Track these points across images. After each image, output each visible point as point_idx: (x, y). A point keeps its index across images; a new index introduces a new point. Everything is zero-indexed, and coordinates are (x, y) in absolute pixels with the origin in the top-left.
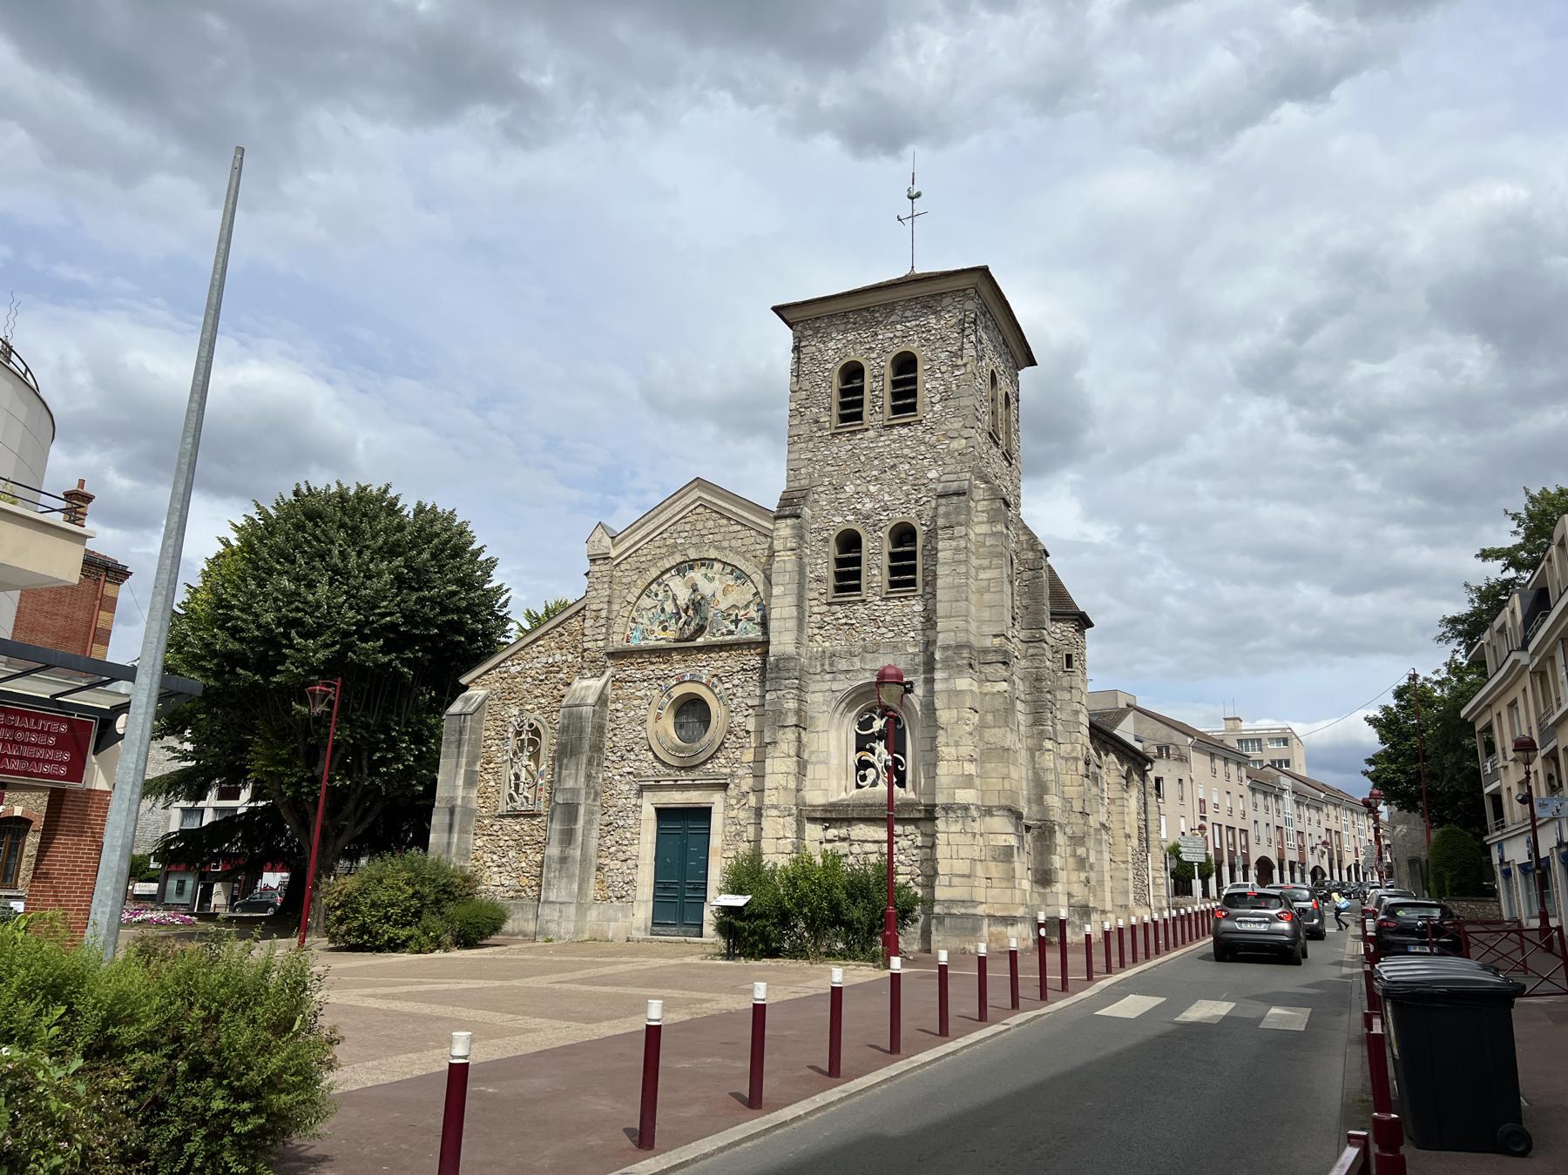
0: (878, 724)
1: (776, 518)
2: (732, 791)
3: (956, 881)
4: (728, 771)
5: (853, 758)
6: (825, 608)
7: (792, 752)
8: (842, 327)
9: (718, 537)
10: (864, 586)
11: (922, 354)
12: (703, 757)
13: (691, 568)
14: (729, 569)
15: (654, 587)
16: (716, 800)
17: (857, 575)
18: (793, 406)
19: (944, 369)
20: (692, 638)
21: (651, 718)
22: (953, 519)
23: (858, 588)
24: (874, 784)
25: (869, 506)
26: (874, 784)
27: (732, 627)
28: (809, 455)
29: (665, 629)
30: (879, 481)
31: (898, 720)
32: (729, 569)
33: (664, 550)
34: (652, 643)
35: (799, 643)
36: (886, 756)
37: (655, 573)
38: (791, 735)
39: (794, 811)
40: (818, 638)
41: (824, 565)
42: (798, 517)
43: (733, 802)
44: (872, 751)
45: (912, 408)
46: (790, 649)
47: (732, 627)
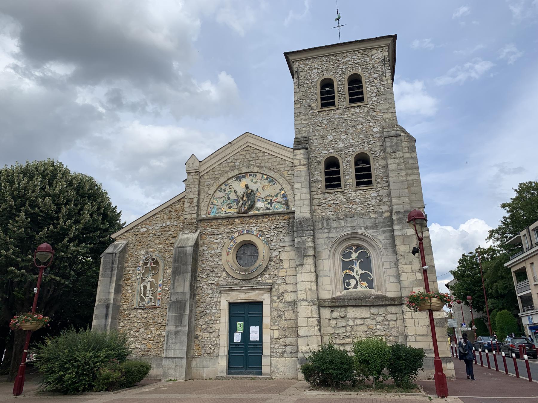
0: (354, 256)
1: (294, 150)
3: (419, 338)
4: (270, 281)
5: (341, 274)
6: (320, 196)
7: (313, 270)
8: (320, 63)
9: (259, 161)
10: (342, 185)
11: (364, 75)
12: (256, 274)
13: (244, 177)
14: (265, 177)
15: (223, 187)
16: (265, 298)
17: (339, 179)
18: (296, 99)
19: (376, 81)
20: (246, 212)
21: (224, 254)
22: (395, 148)
23: (339, 186)
24: (355, 287)
25: (341, 145)
26: (355, 287)
27: (269, 206)
28: (307, 122)
29: (230, 207)
30: (344, 134)
31: (365, 253)
32: (265, 177)
33: (229, 168)
34: (223, 215)
35: (312, 211)
36: (361, 272)
37: (223, 179)
38: (310, 261)
39: (317, 302)
40: (319, 211)
41: (320, 175)
42: (307, 149)
43: (275, 298)
44: (352, 269)
45: (362, 100)
46: (308, 215)
47: (269, 206)
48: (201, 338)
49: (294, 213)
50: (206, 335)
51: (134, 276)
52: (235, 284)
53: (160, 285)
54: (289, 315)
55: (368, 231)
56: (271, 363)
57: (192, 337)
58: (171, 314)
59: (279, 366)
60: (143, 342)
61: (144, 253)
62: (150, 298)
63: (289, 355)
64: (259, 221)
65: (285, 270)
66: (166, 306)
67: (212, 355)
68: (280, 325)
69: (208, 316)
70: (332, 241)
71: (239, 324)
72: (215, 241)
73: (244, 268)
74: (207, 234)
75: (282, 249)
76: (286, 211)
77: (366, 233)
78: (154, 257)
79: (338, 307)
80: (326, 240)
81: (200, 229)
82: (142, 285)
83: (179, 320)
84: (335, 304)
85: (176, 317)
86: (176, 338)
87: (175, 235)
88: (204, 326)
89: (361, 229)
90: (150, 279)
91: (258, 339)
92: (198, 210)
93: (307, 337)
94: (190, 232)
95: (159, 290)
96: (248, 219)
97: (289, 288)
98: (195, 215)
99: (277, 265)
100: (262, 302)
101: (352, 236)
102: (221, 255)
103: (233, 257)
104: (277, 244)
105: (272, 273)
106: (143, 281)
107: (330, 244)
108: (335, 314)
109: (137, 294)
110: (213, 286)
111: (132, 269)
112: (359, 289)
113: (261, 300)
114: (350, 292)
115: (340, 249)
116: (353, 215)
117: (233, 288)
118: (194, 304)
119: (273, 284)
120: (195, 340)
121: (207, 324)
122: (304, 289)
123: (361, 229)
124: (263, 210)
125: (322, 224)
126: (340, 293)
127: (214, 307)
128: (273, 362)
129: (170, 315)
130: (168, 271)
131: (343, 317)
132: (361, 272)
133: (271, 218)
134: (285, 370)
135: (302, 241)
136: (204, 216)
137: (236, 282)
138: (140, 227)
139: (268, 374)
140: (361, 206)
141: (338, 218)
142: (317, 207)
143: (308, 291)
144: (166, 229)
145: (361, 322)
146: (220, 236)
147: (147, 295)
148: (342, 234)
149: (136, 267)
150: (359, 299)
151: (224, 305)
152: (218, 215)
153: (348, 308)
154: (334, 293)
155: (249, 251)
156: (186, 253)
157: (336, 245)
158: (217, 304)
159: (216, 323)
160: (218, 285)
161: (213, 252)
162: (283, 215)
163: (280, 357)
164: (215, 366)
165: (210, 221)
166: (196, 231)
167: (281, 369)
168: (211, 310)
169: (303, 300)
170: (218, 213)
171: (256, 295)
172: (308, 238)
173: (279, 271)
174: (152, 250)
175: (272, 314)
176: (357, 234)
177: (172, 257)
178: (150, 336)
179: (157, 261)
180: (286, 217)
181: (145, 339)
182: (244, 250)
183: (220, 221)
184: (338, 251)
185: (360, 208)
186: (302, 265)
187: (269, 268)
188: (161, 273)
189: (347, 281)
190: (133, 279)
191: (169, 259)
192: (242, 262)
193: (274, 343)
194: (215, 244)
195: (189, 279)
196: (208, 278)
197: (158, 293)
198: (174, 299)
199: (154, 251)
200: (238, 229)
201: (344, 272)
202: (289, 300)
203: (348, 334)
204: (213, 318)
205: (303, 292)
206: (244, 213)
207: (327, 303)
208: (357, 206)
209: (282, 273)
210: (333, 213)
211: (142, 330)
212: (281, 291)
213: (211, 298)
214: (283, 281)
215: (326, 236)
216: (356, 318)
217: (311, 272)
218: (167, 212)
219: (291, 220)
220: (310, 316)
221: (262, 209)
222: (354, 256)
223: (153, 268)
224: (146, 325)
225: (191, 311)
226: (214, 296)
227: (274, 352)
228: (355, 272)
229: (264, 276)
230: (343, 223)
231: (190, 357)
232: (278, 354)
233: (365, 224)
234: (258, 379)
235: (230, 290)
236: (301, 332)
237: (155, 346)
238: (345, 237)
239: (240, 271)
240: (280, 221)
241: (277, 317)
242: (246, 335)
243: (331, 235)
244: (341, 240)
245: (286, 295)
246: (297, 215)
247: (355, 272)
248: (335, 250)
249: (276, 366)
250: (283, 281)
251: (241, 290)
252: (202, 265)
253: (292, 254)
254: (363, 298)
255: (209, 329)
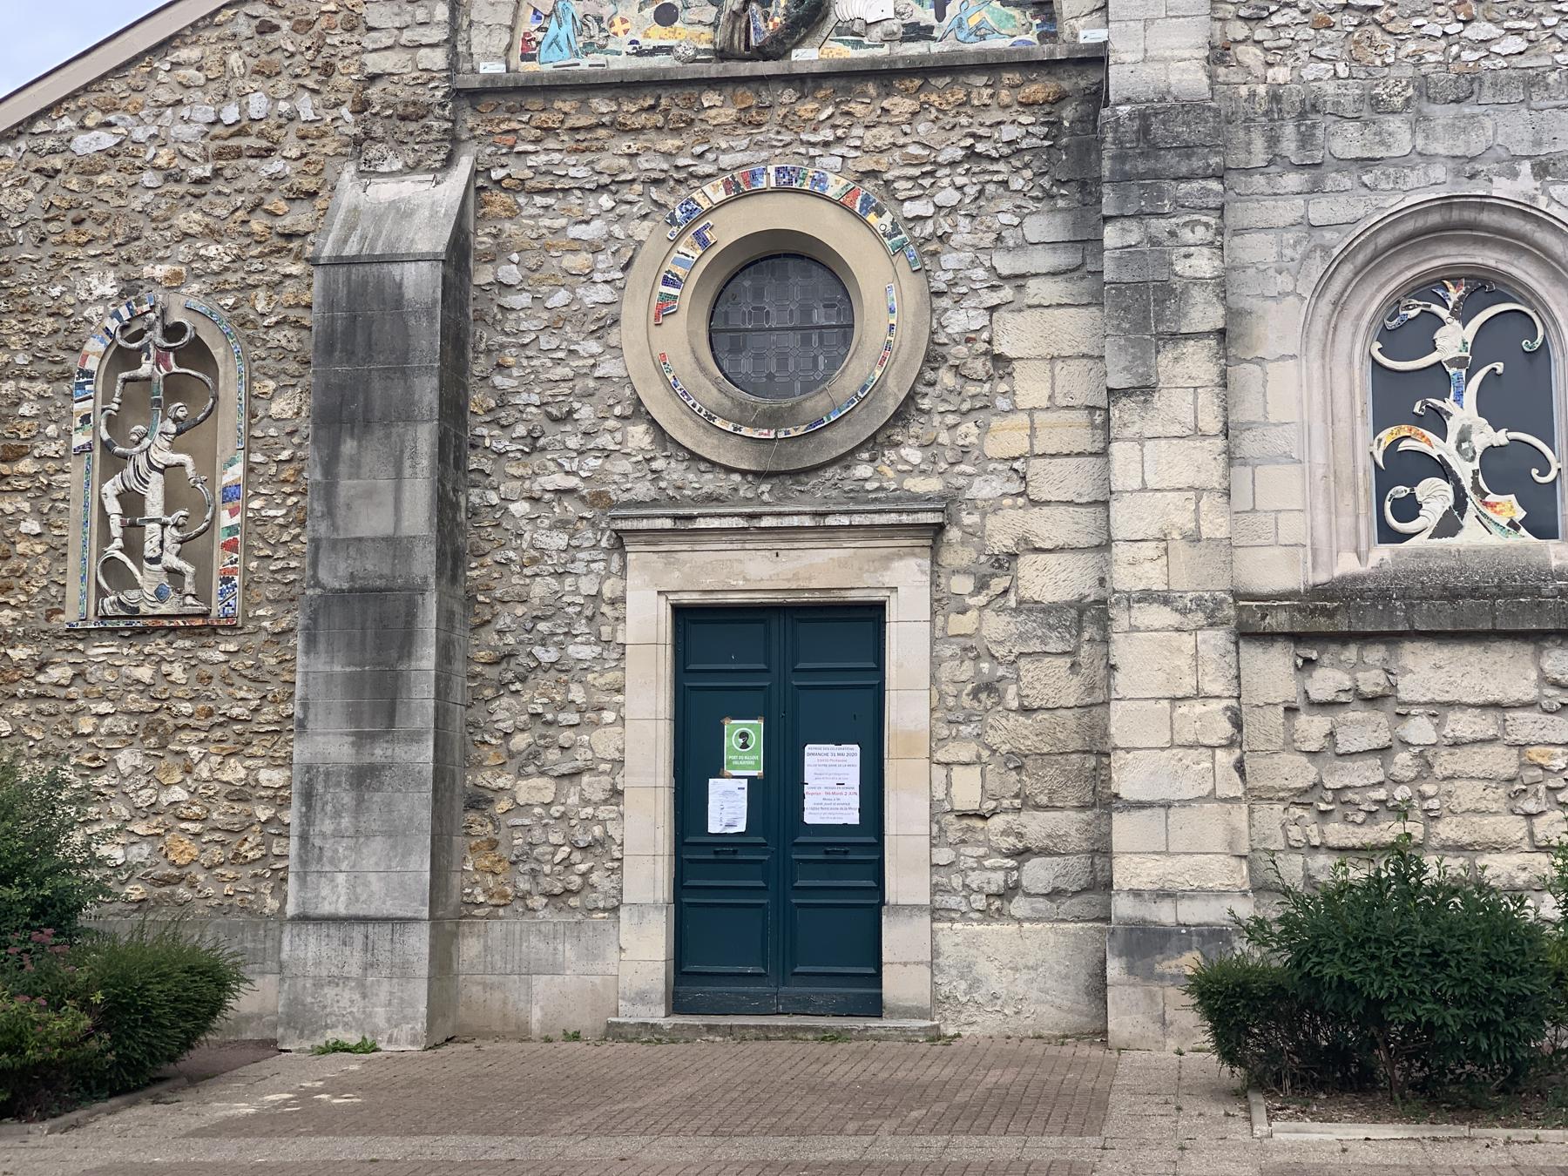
0: (1453, 340)
2: (957, 553)
4: (932, 485)
5: (1370, 447)
7: (1212, 424)
12: (841, 439)
16: (904, 586)
20: (777, 48)
24: (1448, 526)
26: (1448, 526)
34: (622, 63)
36: (1486, 436)
44: (1436, 422)
46: (1190, 78)
48: (503, 805)
49: (1097, 59)
50: (535, 789)
51: (51, 430)
52: (711, 499)
53: (229, 494)
54: (1051, 681)
55: (1557, 191)
56: (935, 952)
57: (457, 802)
58: (321, 665)
59: (983, 968)
60: (140, 828)
61: (108, 288)
62: (172, 572)
63: (1042, 904)
64: (857, 108)
65: (1023, 419)
66: (274, 618)
67: (577, 895)
68: (993, 738)
69: (545, 680)
70: (1326, 250)
71: (733, 729)
72: (575, 231)
73: (765, 404)
74: (521, 187)
75: (1007, 293)
76: (1042, 51)
77: (1542, 203)
78: (176, 317)
79: (1344, 639)
80: (1290, 237)
81: (473, 148)
82: (111, 488)
83: (377, 702)
84: (1323, 622)
85: (354, 684)
86: (360, 806)
87: (309, 184)
88: (520, 741)
89: (1514, 175)
90: (163, 456)
91: (854, 818)
92: (454, 26)
93: (1167, 805)
94: (411, 169)
95: (226, 519)
96: (788, 95)
97: (1051, 527)
98: (437, 59)
99: (972, 389)
100: (880, 607)
101: (1455, 215)
102: (612, 315)
103: (690, 333)
104: (974, 263)
105: (944, 438)
106: (113, 462)
107: (1317, 268)
108: (1327, 681)
109: (78, 537)
110: (572, 508)
111: (39, 386)
112: (1472, 535)
113: (877, 596)
114: (1418, 555)
115: (1371, 301)
116: (1467, 87)
117: (701, 523)
118: (457, 608)
119: (949, 502)
120: (472, 816)
121: (539, 729)
122: (1154, 531)
123: (1514, 175)
124: (889, 38)
125: (1273, 141)
126: (1357, 558)
127: (581, 627)
128: (945, 944)
129: (316, 671)
130: (276, 408)
131: (1372, 701)
132: (1486, 436)
133: (944, 93)
134: (1020, 989)
135: (1154, 241)
136: (498, 68)
137: (711, 483)
138: (67, 123)
139: (922, 1014)
140: (1519, 32)
141: (1376, 103)
142: (1239, 30)
143: (1180, 548)
144: (243, 142)
145: (1484, 725)
146: (606, 201)
147: (150, 549)
148: (1396, 203)
149: (66, 376)
150: (1474, 592)
151: (646, 622)
152: (585, 64)
153: (1408, 647)
154: (1323, 558)
155: (784, 300)
156: (399, 300)
157: (1347, 270)
158: (602, 610)
159: (596, 724)
160: (599, 499)
161: (560, 298)
162: (1016, 77)
163: (986, 915)
164: (599, 967)
165: (535, 103)
166: (449, 162)
167: (995, 980)
168: (561, 646)
169: (1147, 597)
170: (589, 48)
171: (843, 564)
172: (1192, 225)
173: (984, 429)
174: (160, 271)
175: (945, 673)
176: (1483, 203)
177: (297, 325)
178: (179, 794)
179: (197, 340)
180: (1038, 89)
181: (153, 810)
182: (758, 294)
183: (602, 105)
184: (1354, 308)
185: (1515, 44)
186: (1145, 390)
187: (925, 404)
188: (230, 419)
189: (1401, 491)
190: (50, 449)
191: (281, 337)
192: (746, 365)
193: (952, 836)
194: (576, 247)
195: (425, 462)
196: (536, 460)
197: (221, 538)
198: (335, 574)
199: (175, 282)
200: (726, 160)
201: (1387, 436)
202: (1049, 598)
203: (1402, 792)
204: (577, 694)
205: (1149, 549)
206: (762, 54)
207: (1283, 616)
208: (1496, 31)
209: (1007, 438)
210: (1342, 70)
211: (127, 759)
212: (1001, 541)
213: (558, 575)
214: (1016, 487)
215: (1290, 217)
216: (1450, 705)
217: (1198, 433)
218: (244, 28)
219: (1068, 113)
220: (1188, 690)
221: (876, 33)
222: (1453, 340)
223: (175, 388)
224: (155, 730)
225: (445, 653)
226: (579, 567)
227: (952, 891)
228: (1452, 436)
229: (891, 454)
230: (1400, 136)
231: (448, 916)
232: (979, 902)
233: (1538, 143)
234: (862, 1035)
235: (684, 530)
236: (1128, 780)
237: (217, 854)
238: (1409, 226)
239: (741, 422)
240: (995, 115)
241: (975, 694)
242: (778, 790)
243: (1321, 211)
244: (1384, 239)
245: (1027, 566)
246: (1120, 79)
247: (1452, 436)
248: (1339, 305)
249: (966, 970)
250: (1016, 487)
251: (750, 532)
252: (498, 380)
253: (1074, 327)
254: (1501, 591)
255: (553, 755)
